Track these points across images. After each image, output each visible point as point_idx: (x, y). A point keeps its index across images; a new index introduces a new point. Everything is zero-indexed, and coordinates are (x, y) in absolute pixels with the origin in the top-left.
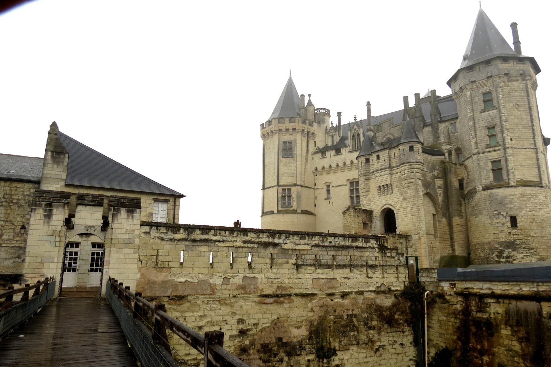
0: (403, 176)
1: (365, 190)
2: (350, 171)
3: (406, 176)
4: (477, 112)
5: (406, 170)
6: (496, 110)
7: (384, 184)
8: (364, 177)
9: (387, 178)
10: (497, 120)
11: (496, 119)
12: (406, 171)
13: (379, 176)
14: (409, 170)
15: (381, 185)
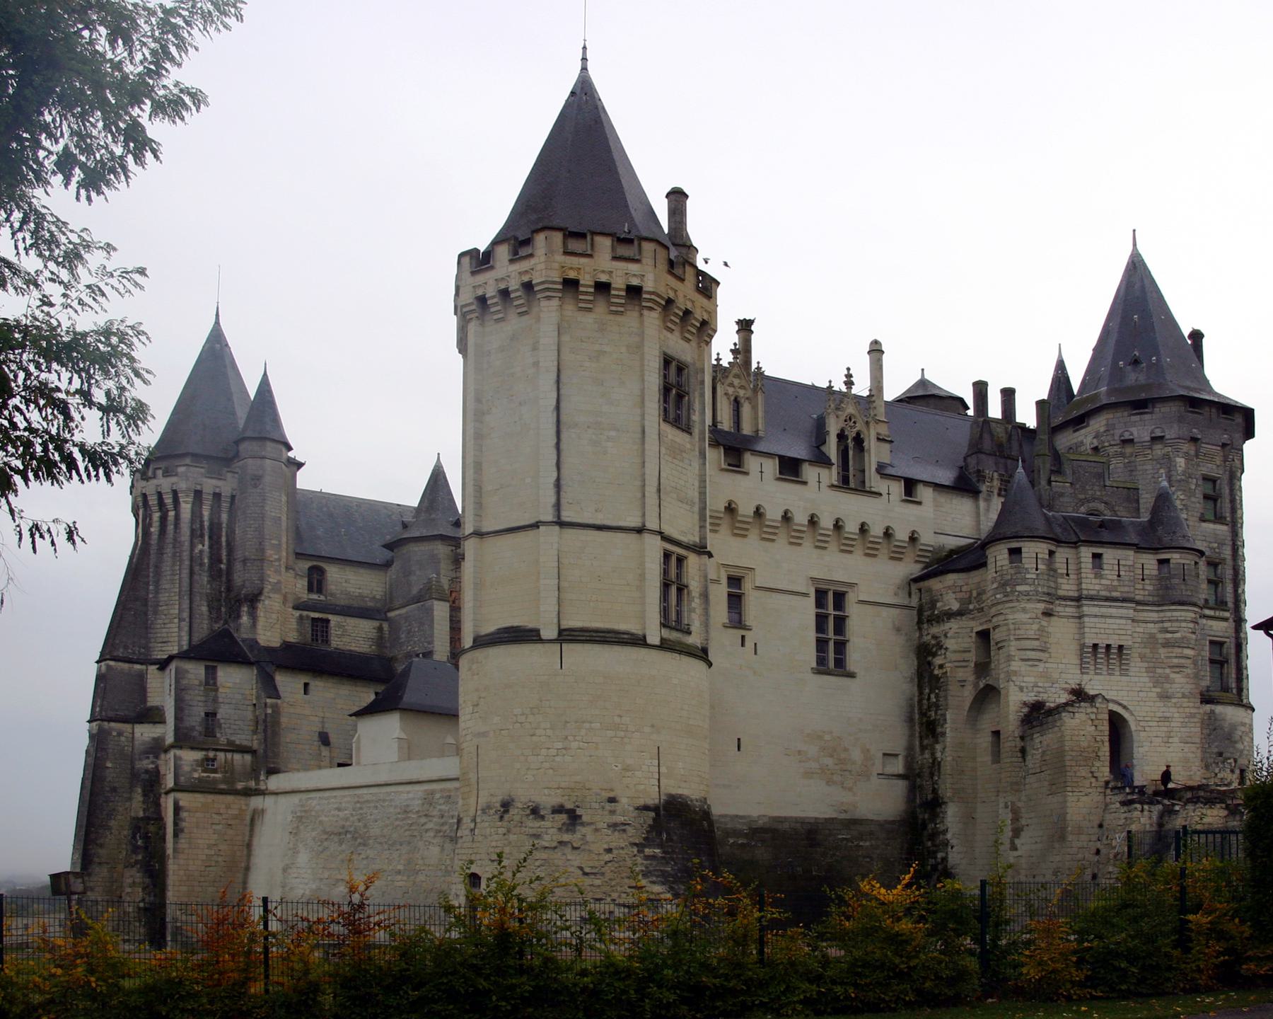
0: (1169, 636)
1: (1036, 644)
2: (819, 551)
3: (1183, 638)
4: (1193, 516)
5: (1185, 621)
6: (1225, 528)
7: (1115, 642)
8: (1042, 606)
9: (1122, 627)
10: (1227, 552)
11: (1224, 547)
12: (1184, 624)
13: (1096, 616)
14: (1191, 625)
15: (1102, 643)
